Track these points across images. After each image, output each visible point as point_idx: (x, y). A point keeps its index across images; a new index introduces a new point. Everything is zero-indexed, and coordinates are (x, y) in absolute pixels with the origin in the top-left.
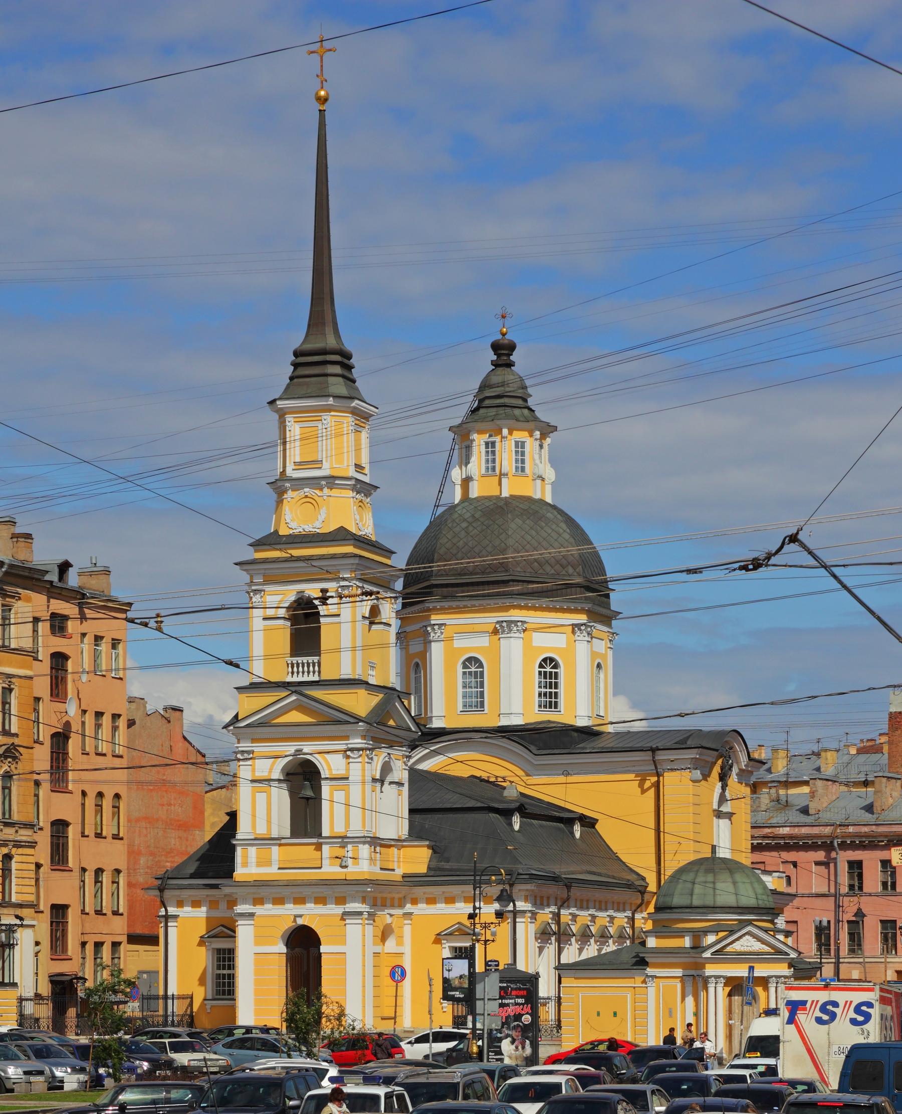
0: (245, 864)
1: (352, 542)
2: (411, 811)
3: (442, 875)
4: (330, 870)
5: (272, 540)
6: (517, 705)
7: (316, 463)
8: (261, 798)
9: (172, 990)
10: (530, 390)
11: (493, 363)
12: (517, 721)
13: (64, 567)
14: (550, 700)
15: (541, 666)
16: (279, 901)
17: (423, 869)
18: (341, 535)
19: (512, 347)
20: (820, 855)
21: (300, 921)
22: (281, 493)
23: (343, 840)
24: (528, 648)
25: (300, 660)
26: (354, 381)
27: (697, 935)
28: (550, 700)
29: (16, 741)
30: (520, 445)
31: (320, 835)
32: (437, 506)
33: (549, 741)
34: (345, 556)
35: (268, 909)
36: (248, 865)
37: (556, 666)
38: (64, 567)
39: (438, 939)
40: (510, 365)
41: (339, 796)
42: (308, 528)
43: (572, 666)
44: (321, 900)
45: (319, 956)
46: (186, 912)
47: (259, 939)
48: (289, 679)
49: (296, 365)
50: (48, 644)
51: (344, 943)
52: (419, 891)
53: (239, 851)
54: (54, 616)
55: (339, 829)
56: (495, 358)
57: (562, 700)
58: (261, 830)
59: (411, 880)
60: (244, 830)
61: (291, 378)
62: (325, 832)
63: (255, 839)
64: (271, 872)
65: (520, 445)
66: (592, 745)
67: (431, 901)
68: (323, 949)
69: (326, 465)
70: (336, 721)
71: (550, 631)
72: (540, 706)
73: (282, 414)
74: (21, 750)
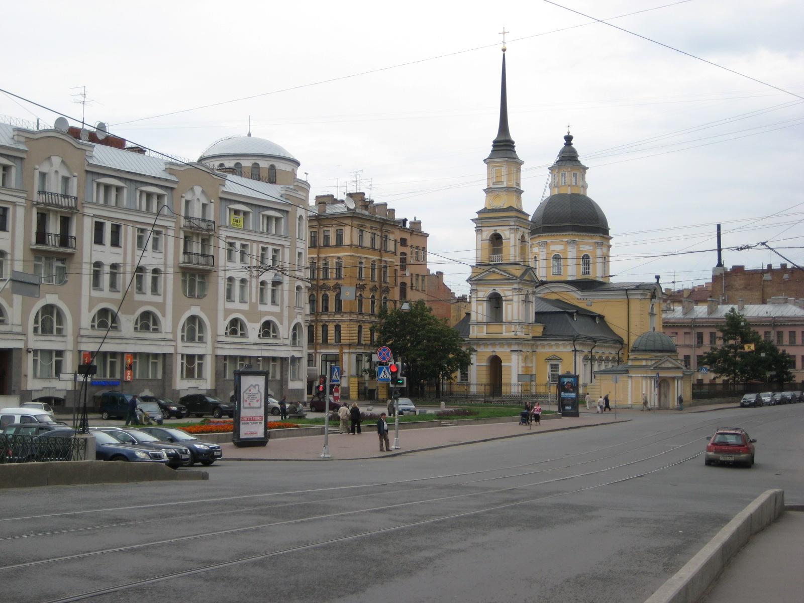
0: (473, 332)
1: (515, 212)
2: (536, 313)
3: (546, 336)
4: (505, 335)
6: (572, 272)
7: (502, 182)
8: (480, 307)
9: (656, 375)
10: (578, 154)
11: (565, 144)
12: (575, 278)
13: (405, 221)
14: (586, 271)
15: (583, 258)
16: (486, 345)
17: (540, 335)
18: (510, 209)
20: (687, 330)
21: (494, 354)
24: (578, 251)
25: (497, 255)
26: (515, 152)
28: (586, 271)
29: (389, 286)
31: (501, 321)
32: (543, 197)
33: (586, 285)
34: (512, 217)
35: (481, 349)
37: (589, 258)
38: (405, 221)
39: (547, 360)
40: (571, 144)
41: (509, 307)
44: (502, 345)
45: (501, 367)
47: (478, 360)
48: (491, 263)
49: (494, 146)
50: (401, 249)
51: (510, 363)
52: (539, 343)
53: (471, 327)
54: (402, 239)
55: (509, 319)
56: (565, 142)
57: (591, 271)
58: (480, 319)
59: (535, 339)
60: (473, 317)
61: (492, 151)
62: (504, 320)
63: (477, 323)
64: (483, 335)
66: (600, 288)
67: (543, 346)
68: (503, 364)
69: (505, 183)
70: (509, 280)
71: (587, 244)
72: (582, 273)
74: (390, 289)
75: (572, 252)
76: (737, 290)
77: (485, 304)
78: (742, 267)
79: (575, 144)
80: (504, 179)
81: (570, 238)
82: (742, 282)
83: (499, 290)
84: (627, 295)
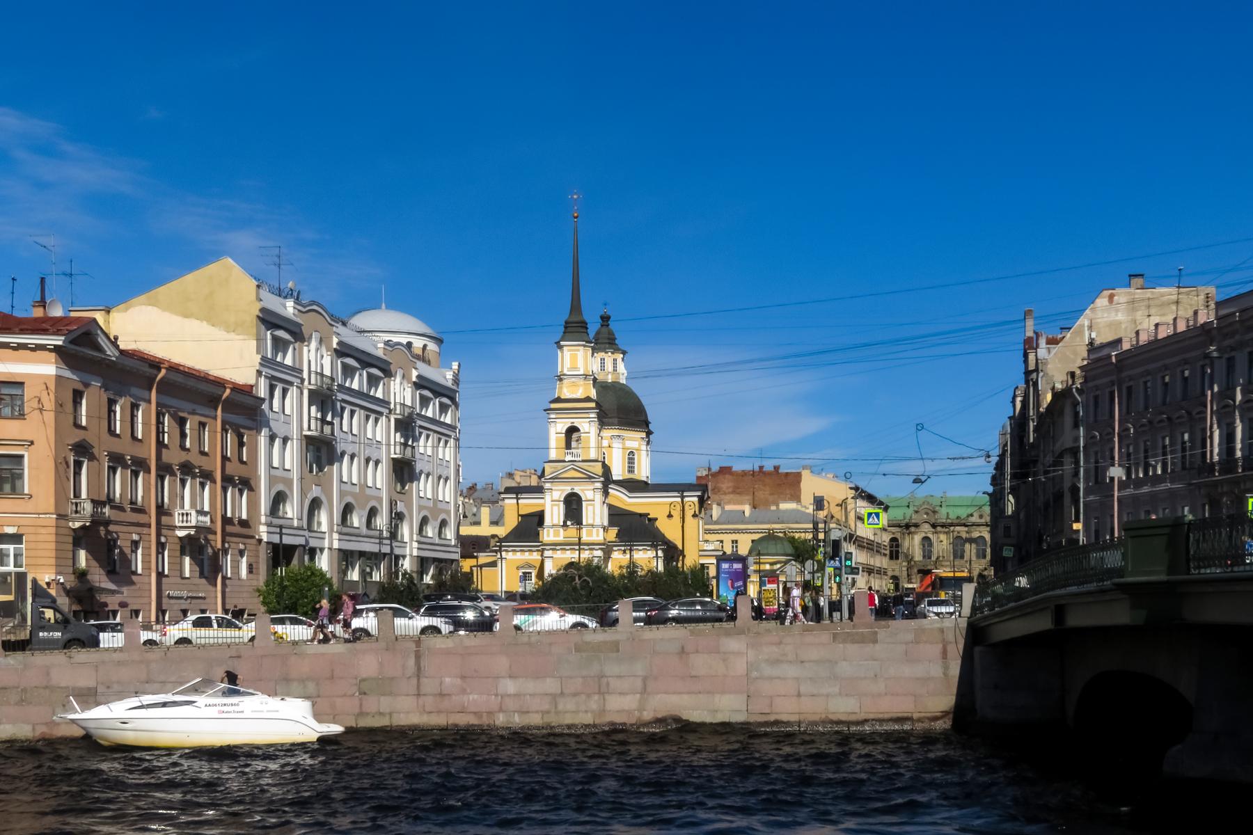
5: (558, 400)
8: (555, 508)
14: (631, 470)
18: (588, 399)
19: (608, 318)
22: (561, 380)
23: (592, 526)
27: (772, 564)
28: (631, 470)
30: (615, 360)
33: (634, 486)
35: (559, 554)
36: (547, 535)
41: (590, 508)
42: (574, 396)
43: (639, 455)
46: (510, 556)
55: (590, 522)
58: (556, 522)
60: (548, 521)
64: (561, 538)
65: (615, 360)
73: (561, 347)
75: (617, 444)
76: (725, 494)
77: (562, 504)
78: (730, 468)
79: (613, 325)
80: (580, 364)
81: (616, 432)
82: (731, 484)
83: (577, 489)
84: (683, 497)
